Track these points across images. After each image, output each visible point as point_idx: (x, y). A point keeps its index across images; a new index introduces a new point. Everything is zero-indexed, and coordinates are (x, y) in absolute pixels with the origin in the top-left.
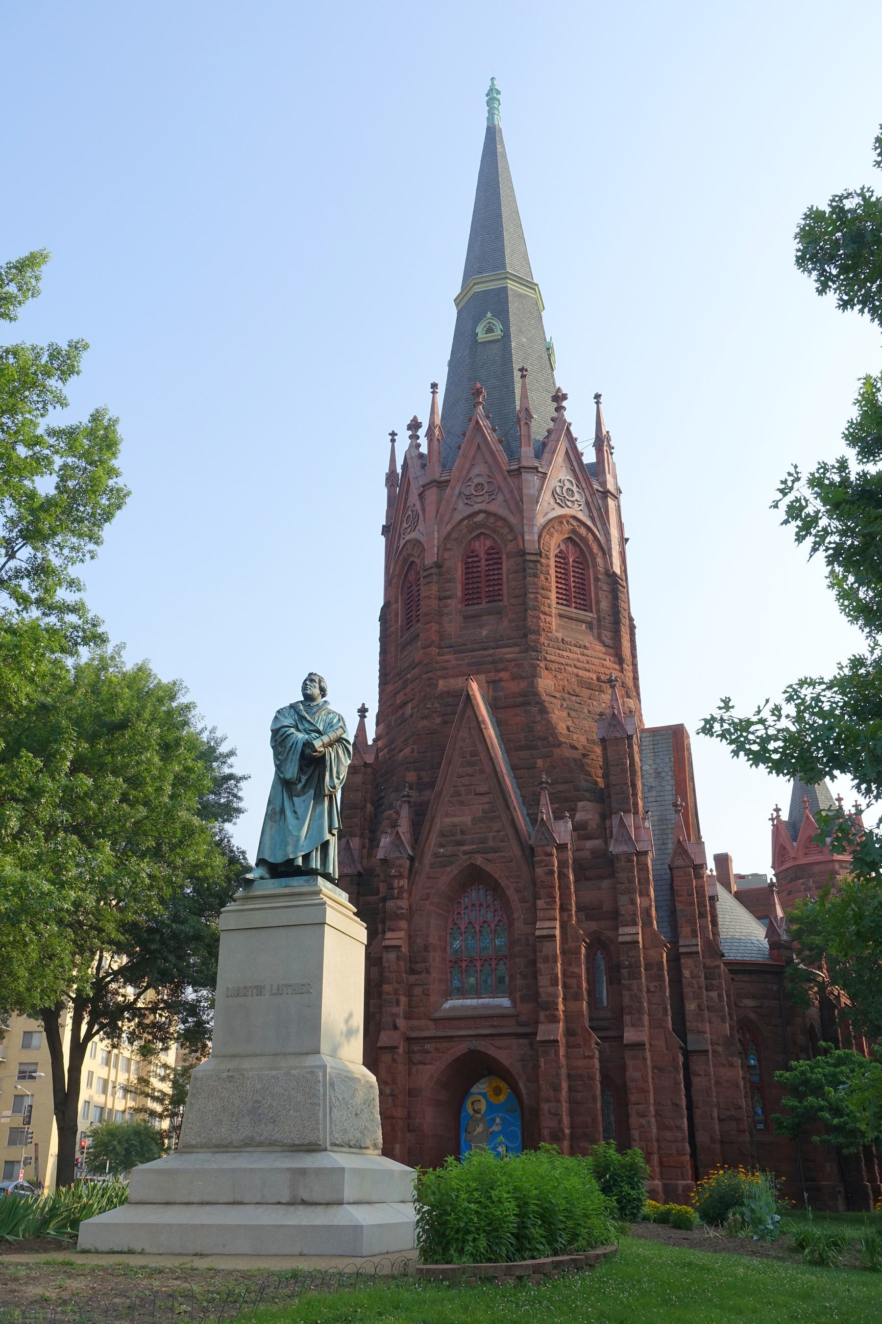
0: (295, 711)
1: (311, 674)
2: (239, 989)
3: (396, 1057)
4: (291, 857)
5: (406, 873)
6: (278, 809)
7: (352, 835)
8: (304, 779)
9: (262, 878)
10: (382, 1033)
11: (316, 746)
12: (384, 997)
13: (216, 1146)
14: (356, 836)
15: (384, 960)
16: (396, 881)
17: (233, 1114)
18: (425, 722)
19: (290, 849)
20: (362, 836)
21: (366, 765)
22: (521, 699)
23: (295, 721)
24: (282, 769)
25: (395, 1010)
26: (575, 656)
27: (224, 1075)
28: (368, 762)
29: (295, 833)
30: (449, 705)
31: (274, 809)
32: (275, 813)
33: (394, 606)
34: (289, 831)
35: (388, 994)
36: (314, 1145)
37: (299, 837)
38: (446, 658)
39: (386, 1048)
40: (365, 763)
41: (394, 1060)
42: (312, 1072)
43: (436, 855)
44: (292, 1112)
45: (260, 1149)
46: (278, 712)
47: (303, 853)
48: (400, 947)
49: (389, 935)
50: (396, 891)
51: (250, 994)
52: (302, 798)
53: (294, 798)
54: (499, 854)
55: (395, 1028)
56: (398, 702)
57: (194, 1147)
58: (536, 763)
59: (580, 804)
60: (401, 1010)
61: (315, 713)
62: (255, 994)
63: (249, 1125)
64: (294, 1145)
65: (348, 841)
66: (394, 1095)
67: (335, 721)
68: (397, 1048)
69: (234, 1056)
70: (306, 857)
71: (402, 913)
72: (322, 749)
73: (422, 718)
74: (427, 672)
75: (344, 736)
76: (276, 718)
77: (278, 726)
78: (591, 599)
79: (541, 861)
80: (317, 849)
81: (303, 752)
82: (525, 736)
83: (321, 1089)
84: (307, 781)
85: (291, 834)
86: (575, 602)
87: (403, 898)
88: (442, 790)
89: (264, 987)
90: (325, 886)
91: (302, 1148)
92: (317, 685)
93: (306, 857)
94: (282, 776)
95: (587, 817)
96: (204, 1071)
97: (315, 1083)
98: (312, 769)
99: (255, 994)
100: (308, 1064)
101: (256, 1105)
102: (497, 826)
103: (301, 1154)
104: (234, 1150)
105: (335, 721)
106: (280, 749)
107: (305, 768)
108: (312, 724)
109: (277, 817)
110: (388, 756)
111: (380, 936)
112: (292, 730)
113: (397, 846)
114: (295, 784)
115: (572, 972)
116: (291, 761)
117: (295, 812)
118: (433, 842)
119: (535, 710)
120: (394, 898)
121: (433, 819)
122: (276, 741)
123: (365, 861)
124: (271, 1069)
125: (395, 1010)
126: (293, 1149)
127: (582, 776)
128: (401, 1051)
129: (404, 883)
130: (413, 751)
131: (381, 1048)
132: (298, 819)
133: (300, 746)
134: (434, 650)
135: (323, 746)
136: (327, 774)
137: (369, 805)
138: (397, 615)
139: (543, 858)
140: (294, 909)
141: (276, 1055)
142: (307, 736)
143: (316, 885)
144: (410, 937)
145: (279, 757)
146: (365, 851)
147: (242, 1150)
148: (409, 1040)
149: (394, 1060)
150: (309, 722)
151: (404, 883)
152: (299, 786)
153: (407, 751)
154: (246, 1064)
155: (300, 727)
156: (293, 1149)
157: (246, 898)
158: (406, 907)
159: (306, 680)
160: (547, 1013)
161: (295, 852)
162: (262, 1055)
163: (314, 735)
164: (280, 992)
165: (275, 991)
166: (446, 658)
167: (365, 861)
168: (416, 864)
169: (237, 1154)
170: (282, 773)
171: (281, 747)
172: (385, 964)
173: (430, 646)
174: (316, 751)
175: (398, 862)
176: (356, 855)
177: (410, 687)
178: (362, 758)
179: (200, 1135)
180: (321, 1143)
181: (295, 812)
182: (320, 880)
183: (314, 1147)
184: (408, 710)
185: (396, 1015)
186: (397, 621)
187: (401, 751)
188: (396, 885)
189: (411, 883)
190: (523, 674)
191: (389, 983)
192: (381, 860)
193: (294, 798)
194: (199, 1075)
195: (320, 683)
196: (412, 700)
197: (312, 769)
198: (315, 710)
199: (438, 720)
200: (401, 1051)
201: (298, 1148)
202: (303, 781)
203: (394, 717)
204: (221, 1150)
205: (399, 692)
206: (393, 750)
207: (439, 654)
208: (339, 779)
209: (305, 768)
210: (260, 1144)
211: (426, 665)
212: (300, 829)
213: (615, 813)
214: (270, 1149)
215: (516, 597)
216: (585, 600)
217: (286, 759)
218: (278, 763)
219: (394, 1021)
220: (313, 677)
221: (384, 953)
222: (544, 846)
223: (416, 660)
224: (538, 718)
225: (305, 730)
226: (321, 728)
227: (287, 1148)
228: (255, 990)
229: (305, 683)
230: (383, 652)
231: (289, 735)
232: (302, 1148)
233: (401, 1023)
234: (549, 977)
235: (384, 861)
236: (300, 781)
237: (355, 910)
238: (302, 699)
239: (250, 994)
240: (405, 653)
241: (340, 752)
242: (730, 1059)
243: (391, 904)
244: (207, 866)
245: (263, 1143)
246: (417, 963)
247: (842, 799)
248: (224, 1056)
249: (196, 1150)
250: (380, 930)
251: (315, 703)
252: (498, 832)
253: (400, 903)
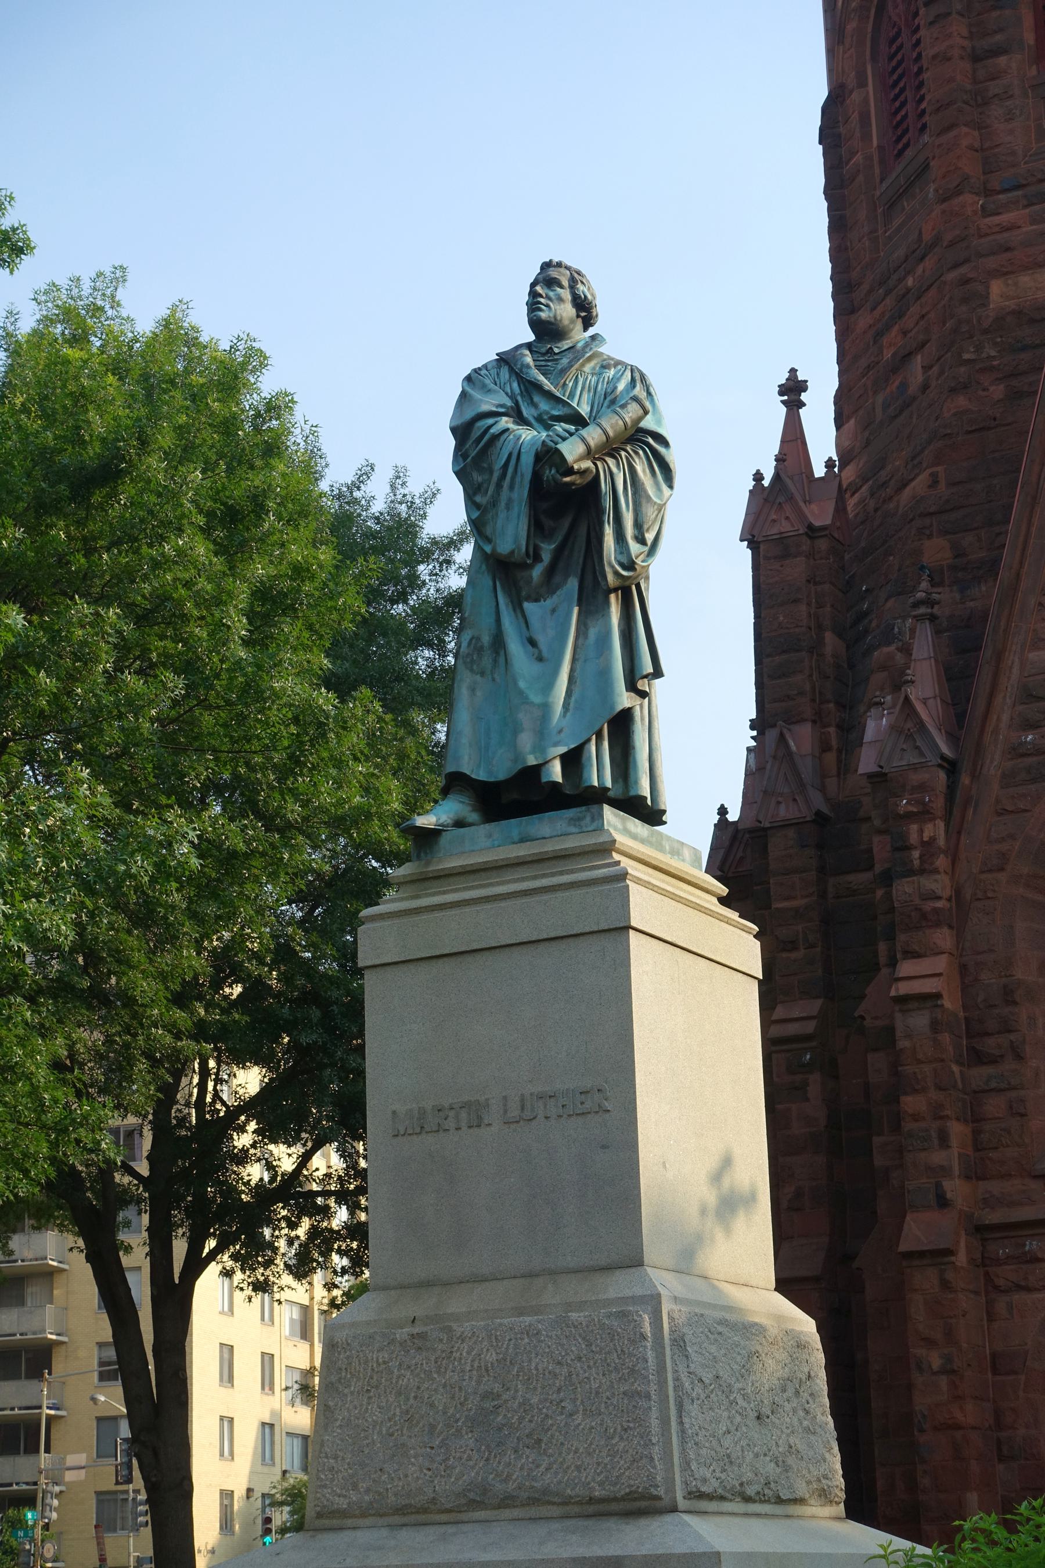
0: (512, 370)
1: (546, 266)
2: (422, 1113)
3: (950, 1275)
4: (532, 761)
5: (939, 804)
6: (486, 639)
7: (792, 719)
8: (547, 551)
9: (459, 824)
10: (908, 1218)
11: (570, 458)
12: (908, 1126)
13: (401, 1510)
14: (803, 720)
15: (899, 1034)
16: (914, 827)
17: (432, 1427)
18: (961, 401)
19: (526, 740)
20: (819, 720)
21: (812, 532)
23: (512, 397)
24: (488, 531)
25: (938, 1157)
27: (402, 1334)
28: (817, 523)
29: (536, 699)
30: (1024, 348)
31: (475, 639)
32: (480, 650)
33: (856, 97)
34: (521, 693)
35: (916, 1117)
36: (643, 1497)
37: (546, 708)
38: (1006, 218)
39: (922, 1254)
40: (810, 527)
41: (945, 1285)
42: (623, 1315)
43: (1017, 751)
44: (579, 1418)
45: (507, 1513)
46: (469, 379)
47: (563, 750)
48: (938, 996)
49: (906, 968)
50: (916, 854)
51: (451, 1124)
52: (549, 603)
53: (526, 605)
55: (943, 1202)
56: (888, 354)
57: (343, 1514)
60: (952, 1157)
61: (564, 371)
62: (463, 1124)
63: (475, 1456)
64: (591, 1500)
65: (782, 735)
66: (953, 1372)
67: (621, 386)
68: (949, 1252)
69: (427, 1284)
70: (573, 760)
71: (936, 911)
72: (587, 464)
73: (953, 390)
74: (956, 266)
75: (648, 423)
76: (464, 395)
77: (469, 415)
80: (599, 735)
81: (536, 477)
83: (650, 1355)
84: (558, 555)
85: (525, 700)
87: (936, 871)
88: (1018, 575)
89: (487, 1105)
90: (626, 832)
91: (614, 1507)
92: (566, 294)
93: (573, 760)
94: (488, 549)
96: (353, 1325)
97: (633, 1342)
98: (566, 523)
99: (463, 1124)
100: (612, 1294)
101: (488, 1405)
103: (611, 1523)
104: (444, 1517)
105: (621, 386)
106: (477, 477)
107: (548, 523)
108: (558, 400)
109: (487, 661)
110: (872, 504)
111: (885, 971)
112: (505, 422)
113: (909, 737)
114: (525, 567)
116: (508, 507)
117: (532, 642)
118: (1005, 718)
120: (911, 872)
121: (999, 656)
122: (465, 456)
123: (832, 783)
124: (520, 1312)
125: (938, 1157)
126: (591, 1509)
128: (961, 1258)
129: (936, 830)
130: (934, 483)
131: (909, 1255)
132: (540, 659)
133: (527, 461)
134: (971, 202)
135: (589, 454)
136: (609, 531)
137: (829, 637)
138: (865, 118)
140: (545, 897)
141: (531, 1275)
142: (544, 434)
143: (600, 829)
144: (963, 969)
145: (478, 499)
146: (831, 758)
147: (464, 1516)
148: (981, 1231)
149: (945, 1285)
150: (549, 395)
151: (936, 830)
153: (919, 484)
154: (456, 1304)
155: (527, 412)
156: (591, 1509)
157: (422, 880)
158: (947, 892)
159: (533, 285)
161: (540, 748)
163: (560, 428)
164: (527, 1114)
165: (514, 1112)
166: (1006, 218)
167: (832, 783)
168: (965, 780)
169: (451, 1529)
170: (489, 540)
171: (481, 470)
172: (903, 1044)
173: (958, 192)
174: (570, 471)
175: (915, 778)
176: (807, 769)
177: (914, 310)
178: (802, 515)
179: (355, 1486)
180: (661, 1492)
181: (532, 642)
182: (609, 814)
183: (643, 1504)
184: (916, 372)
185: (945, 1171)
186: (866, 137)
187: (905, 485)
188: (914, 838)
189: (955, 832)
191: (916, 1091)
192: (870, 776)
193: (526, 605)
195: (573, 287)
196: (923, 345)
197: (566, 523)
198: (565, 361)
199: (998, 391)
200: (961, 1258)
201: (602, 1507)
202: (546, 557)
203: (880, 399)
204: (412, 1518)
205: (888, 327)
206: (885, 484)
207: (985, 212)
208: (642, 541)
209: (548, 523)
210: (507, 1502)
211: (952, 244)
212: (549, 685)
214: (533, 1511)
217: (494, 503)
218: (475, 515)
219: (938, 1186)
220: (553, 273)
221: (898, 1016)
223: (927, 237)
225: (540, 419)
226: (584, 410)
227: (576, 1509)
228: (464, 1115)
229: (533, 294)
230: (838, 227)
231: (496, 437)
232: (614, 1507)
233: (955, 1188)
235: (878, 778)
236: (537, 558)
237: (723, 890)
238: (531, 337)
239: (451, 1124)
240: (896, 223)
241: (640, 467)
243: (904, 889)
244: (369, 816)
245: (513, 1498)
246: (988, 1034)
248: (402, 1287)
249: (349, 1522)
250: (883, 959)
251: (565, 344)
253: (929, 883)
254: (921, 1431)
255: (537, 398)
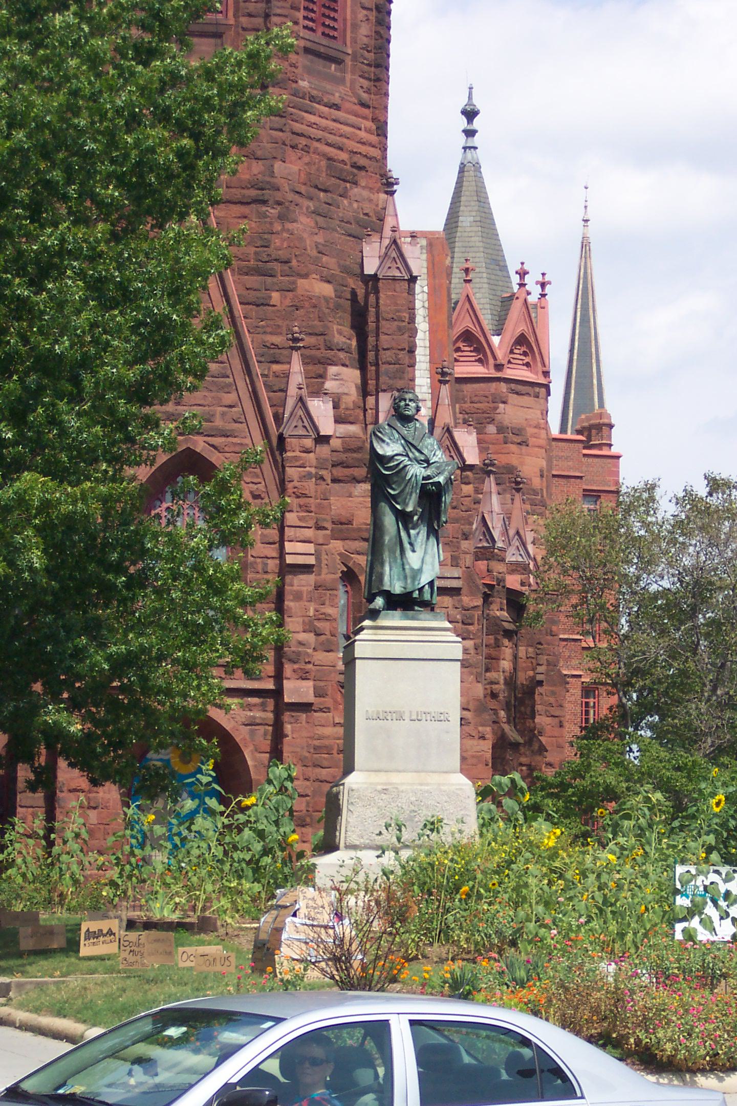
2: (378, 712)
22: (253, 193)
26: (323, 122)
27: (379, 788)
54: (230, 439)
58: (270, 297)
59: (332, 370)
78: (345, 20)
79: (296, 458)
82: (256, 253)
86: (323, 24)
95: (340, 391)
101: (413, 814)
102: (231, 398)
115: (324, 614)
119: (273, 212)
124: (421, 784)
127: (335, 327)
139: (297, 454)
152: (416, 518)
160: (296, 666)
162: (404, 771)
190: (259, 153)
194: (354, 787)
213: (384, 391)
215: (250, 15)
216: (334, 19)
222: (300, 437)
224: (277, 227)
231: (406, 466)
234: (301, 620)
242: (480, 728)
247: (526, 273)
252: (231, 407)
254: (62, 791)
255: (413, 450)
